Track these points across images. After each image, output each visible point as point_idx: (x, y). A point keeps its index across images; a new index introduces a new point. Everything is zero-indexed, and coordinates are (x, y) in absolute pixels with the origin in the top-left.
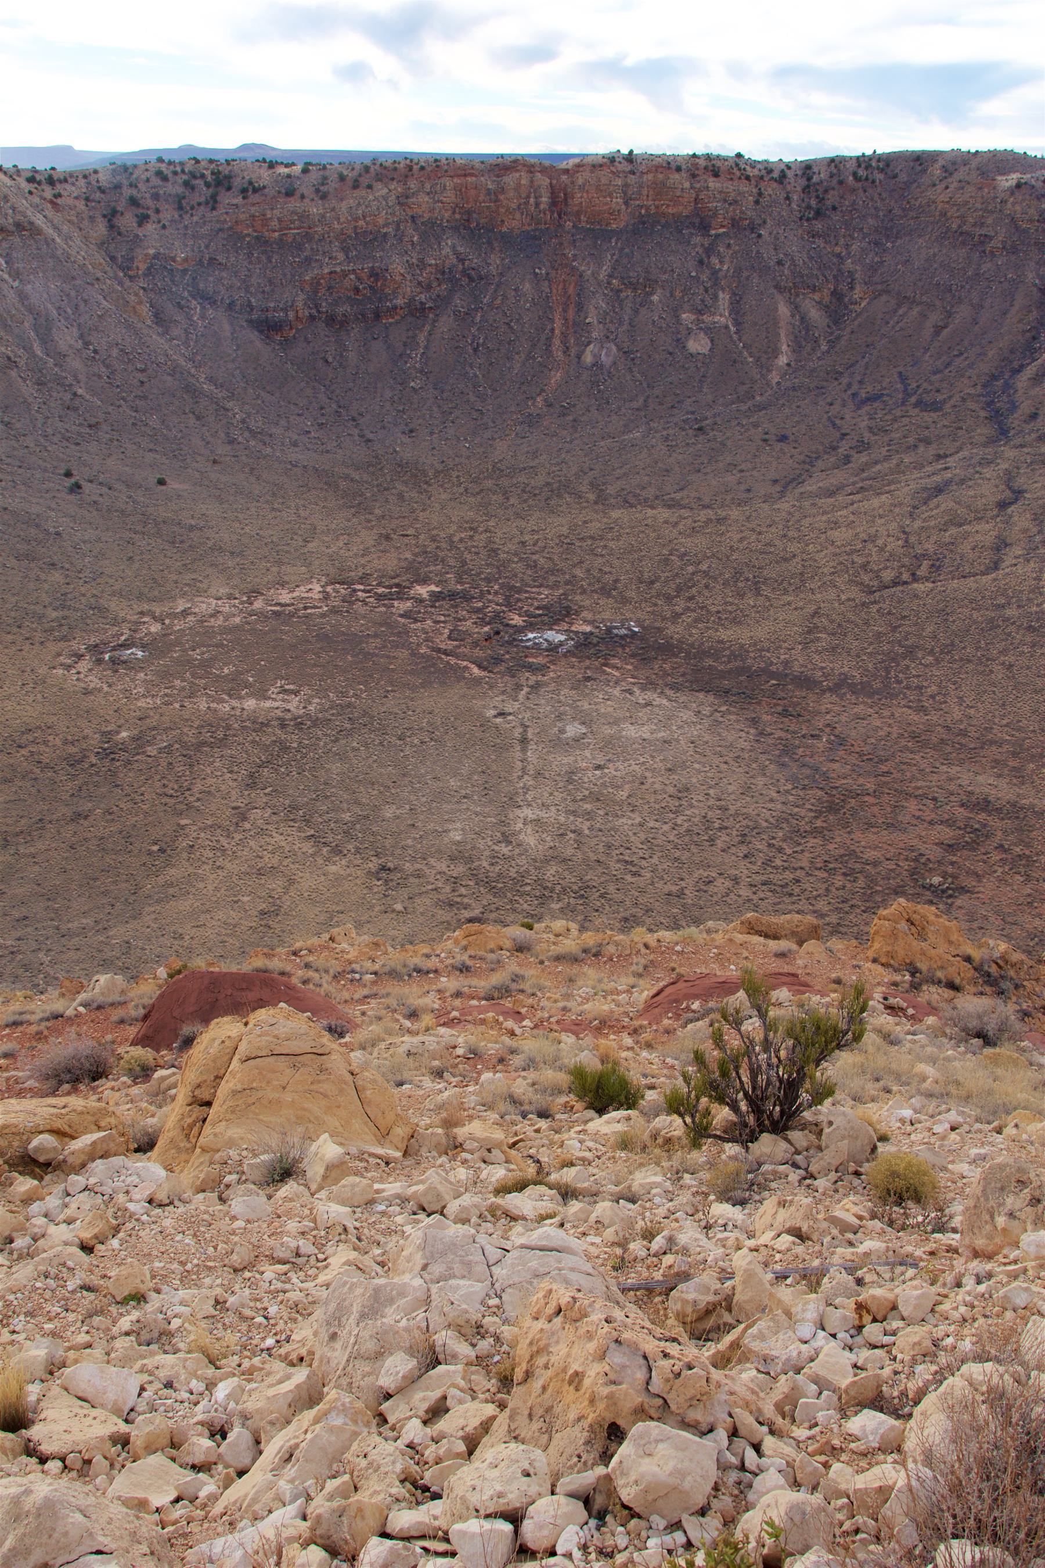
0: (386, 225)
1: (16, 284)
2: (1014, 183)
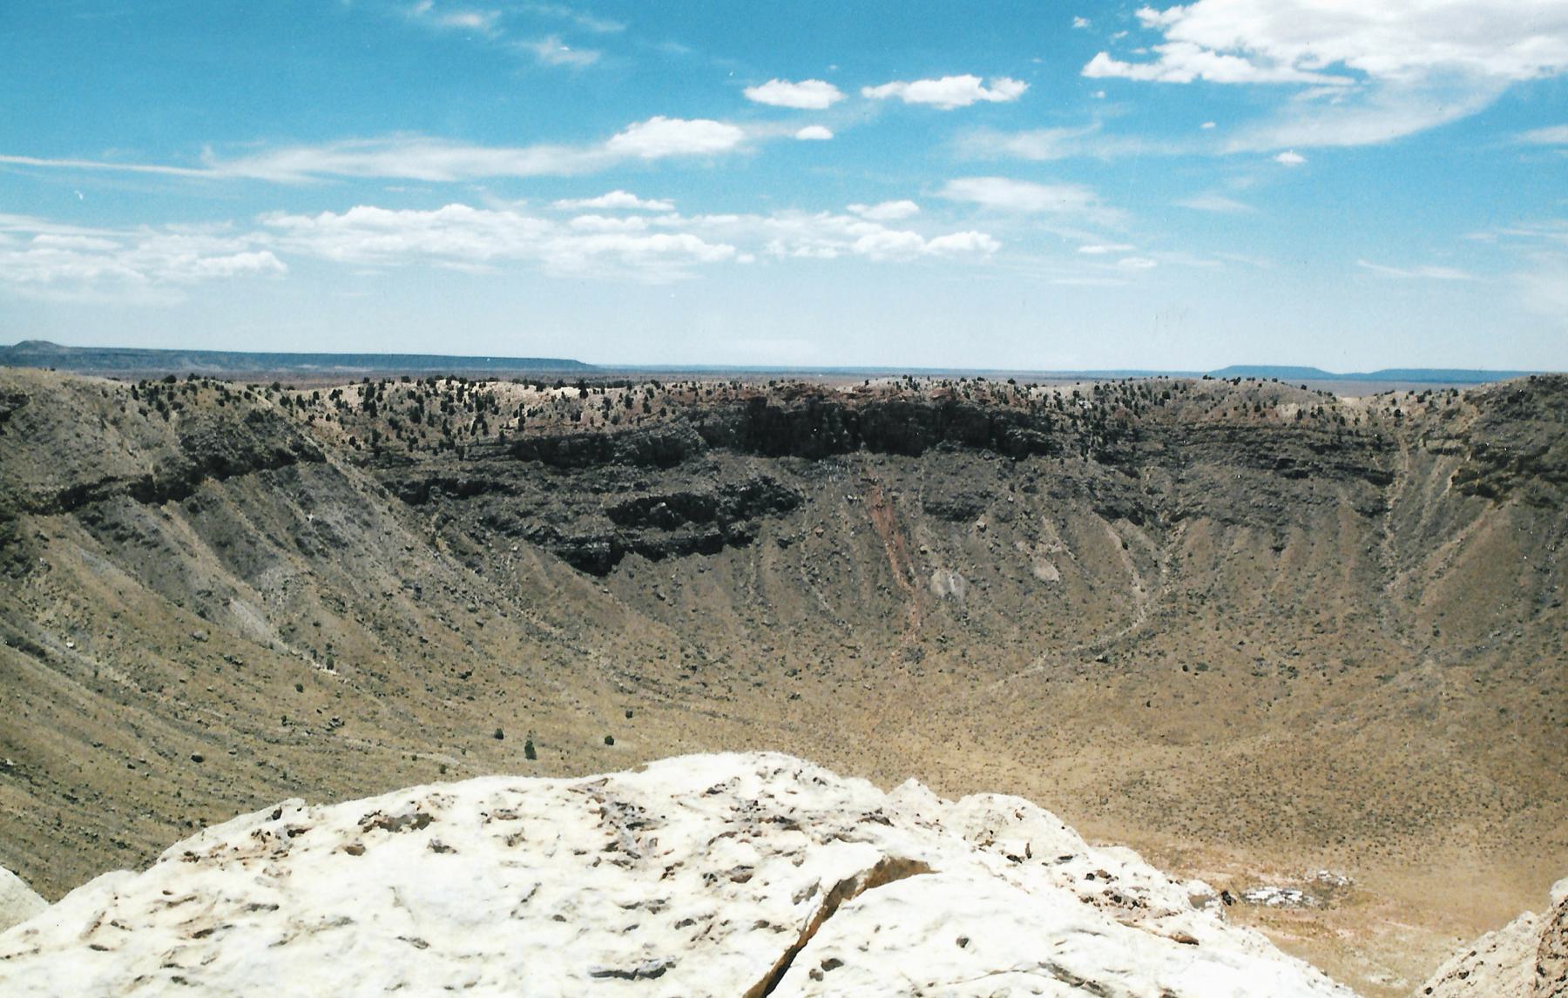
2: (1295, 412)
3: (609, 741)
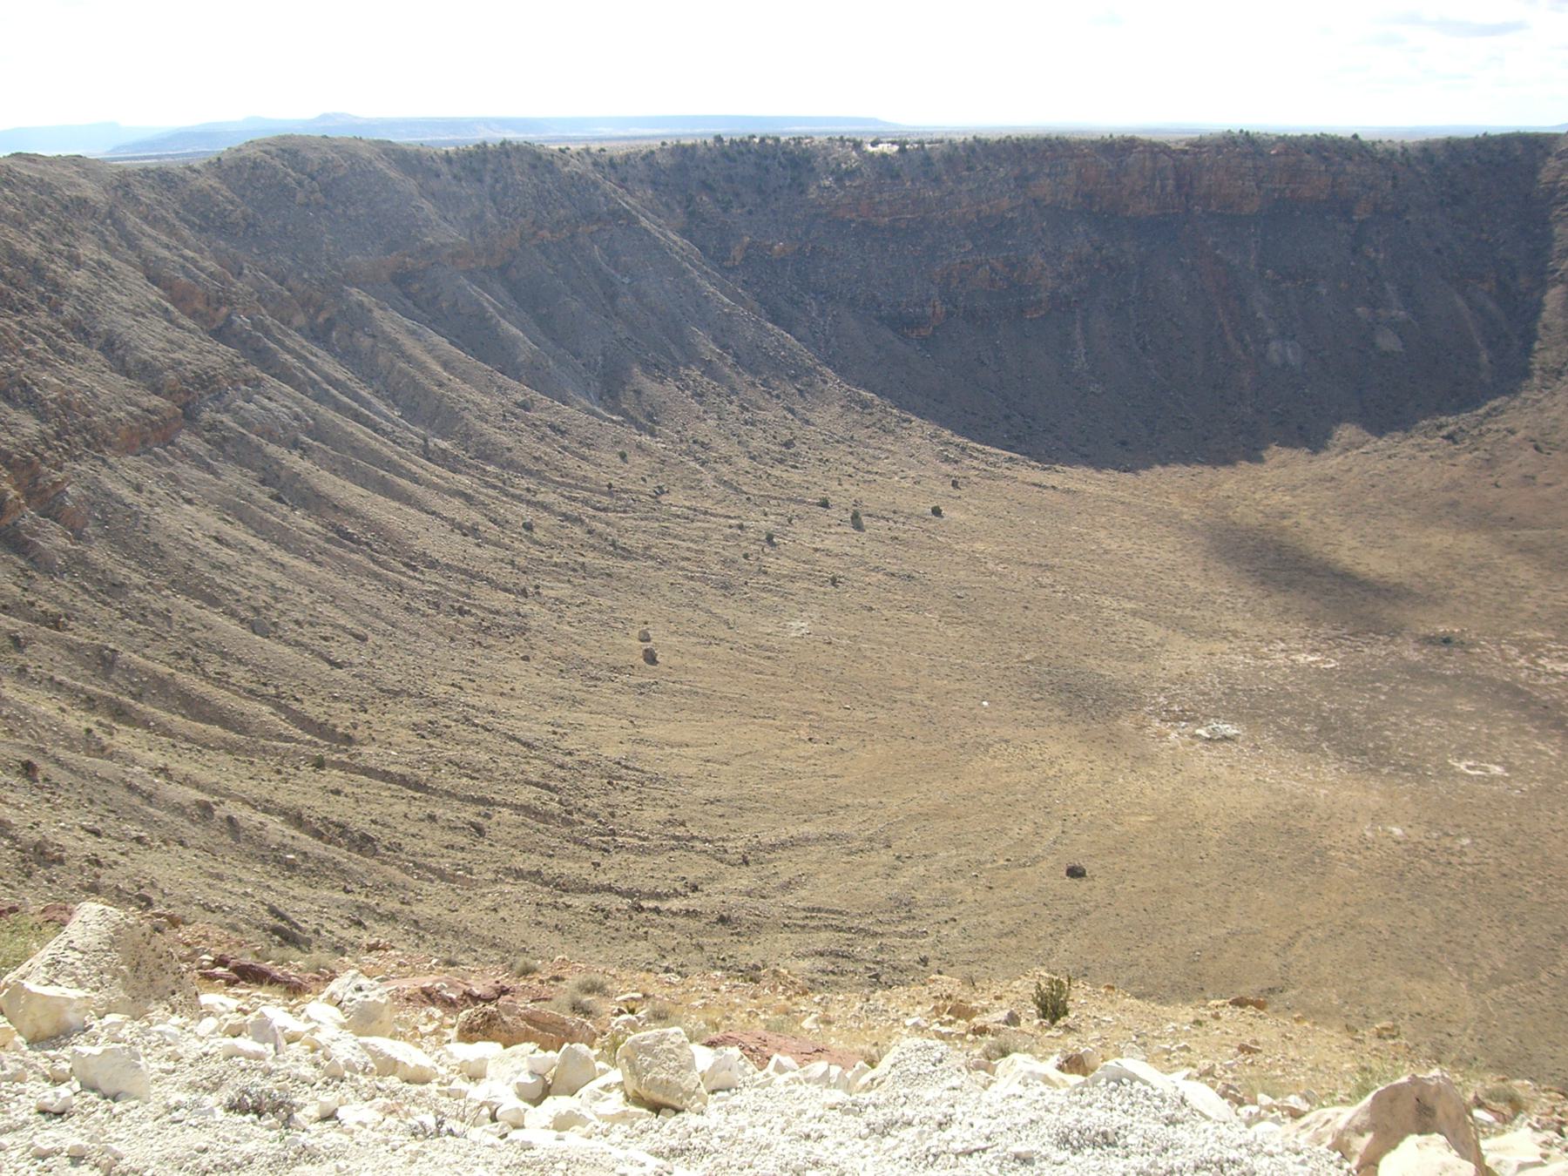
0: (1012, 209)
1: (626, 280)
3: (936, 512)
